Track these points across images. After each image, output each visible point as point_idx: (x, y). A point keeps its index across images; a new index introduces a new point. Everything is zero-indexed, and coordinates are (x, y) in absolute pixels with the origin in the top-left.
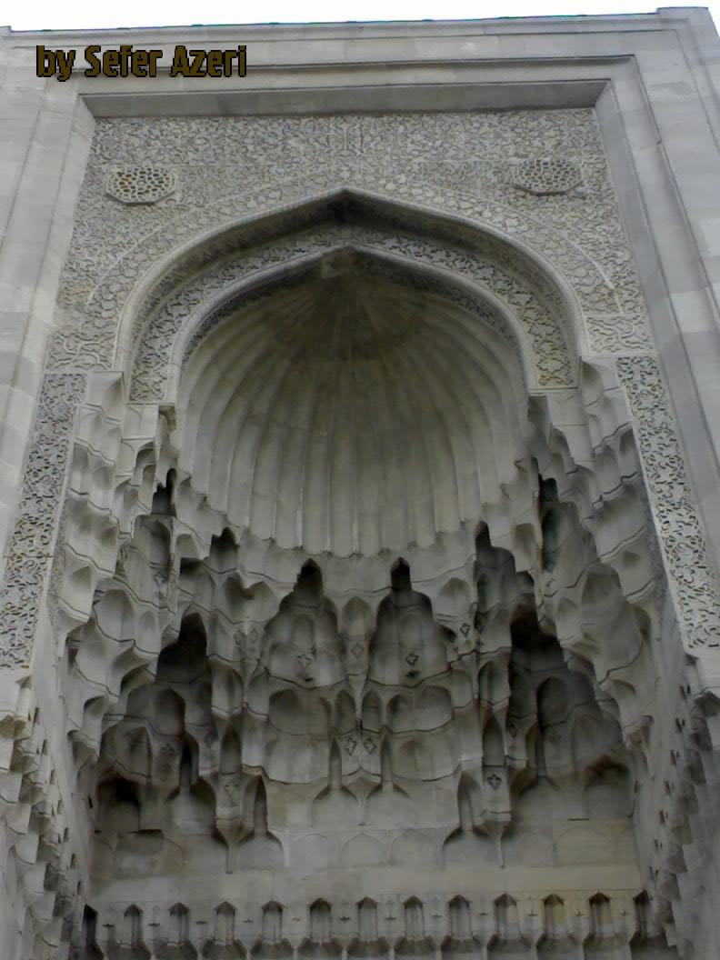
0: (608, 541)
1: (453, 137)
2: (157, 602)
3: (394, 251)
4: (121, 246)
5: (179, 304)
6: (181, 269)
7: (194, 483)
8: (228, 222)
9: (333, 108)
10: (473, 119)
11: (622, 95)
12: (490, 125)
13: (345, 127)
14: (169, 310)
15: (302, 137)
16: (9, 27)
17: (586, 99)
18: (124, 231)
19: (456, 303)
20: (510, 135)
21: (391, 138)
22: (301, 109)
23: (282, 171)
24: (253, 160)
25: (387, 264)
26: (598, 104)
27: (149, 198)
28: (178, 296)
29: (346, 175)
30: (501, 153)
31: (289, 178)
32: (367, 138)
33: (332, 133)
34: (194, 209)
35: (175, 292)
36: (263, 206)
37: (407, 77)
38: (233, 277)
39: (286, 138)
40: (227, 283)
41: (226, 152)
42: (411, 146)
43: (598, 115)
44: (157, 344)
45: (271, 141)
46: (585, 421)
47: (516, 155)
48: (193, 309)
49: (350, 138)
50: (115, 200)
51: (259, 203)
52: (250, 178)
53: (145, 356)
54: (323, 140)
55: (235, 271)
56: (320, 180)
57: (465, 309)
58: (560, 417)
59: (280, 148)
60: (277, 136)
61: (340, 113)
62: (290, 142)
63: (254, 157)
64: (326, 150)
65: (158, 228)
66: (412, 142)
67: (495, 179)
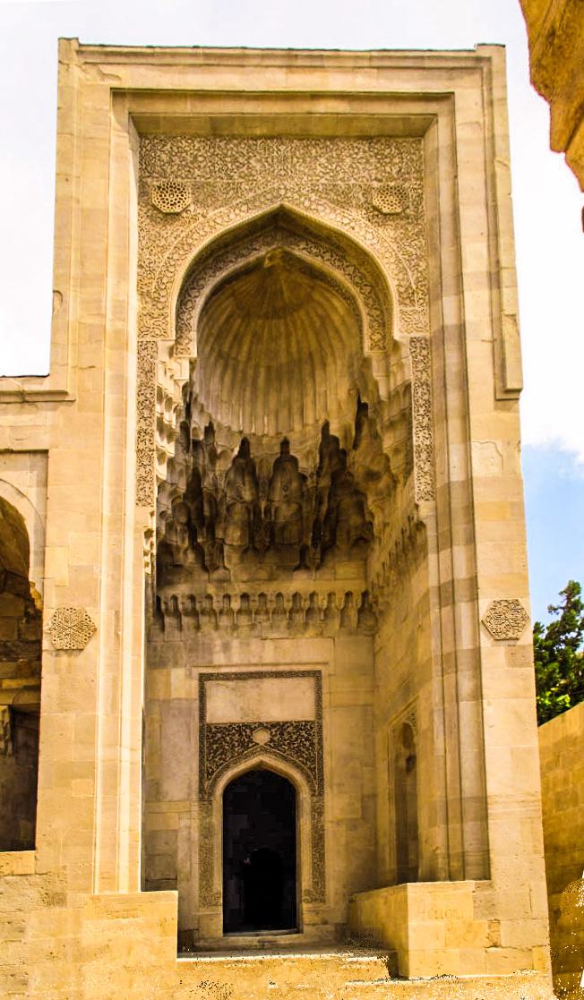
0: (388, 442)
1: (343, 160)
2: (184, 463)
3: (304, 251)
4: (164, 248)
5: (194, 288)
6: (195, 264)
7: (199, 399)
8: (221, 230)
9: (277, 133)
10: (355, 145)
11: (440, 133)
12: (364, 152)
13: (282, 148)
14: (190, 292)
15: (258, 157)
16: (77, 39)
17: (418, 131)
18: (165, 236)
19: (331, 289)
20: (373, 160)
21: (308, 160)
22: (258, 132)
23: (247, 187)
24: (231, 177)
25: (300, 260)
26: (426, 136)
27: (178, 210)
28: (193, 282)
29: (282, 192)
30: (368, 177)
31: (252, 194)
32: (295, 160)
33: (275, 154)
34: (201, 219)
35: (192, 279)
36: (238, 218)
37: (321, 107)
38: (221, 269)
39: (249, 158)
40: (218, 274)
41: (217, 169)
42: (319, 167)
43: (425, 145)
44: (185, 316)
45: (241, 160)
46: (388, 374)
47: (376, 179)
48: (202, 291)
49: (285, 159)
50: (158, 209)
51: (236, 215)
52: (231, 192)
53: (180, 328)
54: (269, 160)
55: (221, 265)
56: (269, 196)
57: (334, 292)
58: (377, 373)
59: (246, 167)
60: (244, 156)
61: (278, 137)
62: (251, 161)
63: (232, 174)
64: (272, 169)
65: (183, 234)
66: (320, 165)
67: (363, 200)
